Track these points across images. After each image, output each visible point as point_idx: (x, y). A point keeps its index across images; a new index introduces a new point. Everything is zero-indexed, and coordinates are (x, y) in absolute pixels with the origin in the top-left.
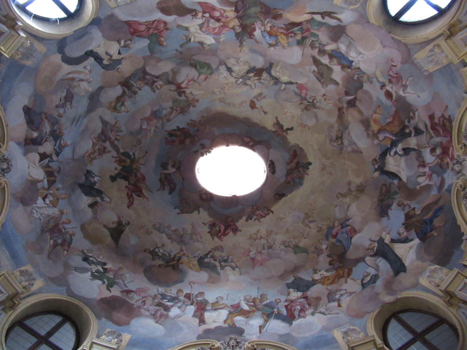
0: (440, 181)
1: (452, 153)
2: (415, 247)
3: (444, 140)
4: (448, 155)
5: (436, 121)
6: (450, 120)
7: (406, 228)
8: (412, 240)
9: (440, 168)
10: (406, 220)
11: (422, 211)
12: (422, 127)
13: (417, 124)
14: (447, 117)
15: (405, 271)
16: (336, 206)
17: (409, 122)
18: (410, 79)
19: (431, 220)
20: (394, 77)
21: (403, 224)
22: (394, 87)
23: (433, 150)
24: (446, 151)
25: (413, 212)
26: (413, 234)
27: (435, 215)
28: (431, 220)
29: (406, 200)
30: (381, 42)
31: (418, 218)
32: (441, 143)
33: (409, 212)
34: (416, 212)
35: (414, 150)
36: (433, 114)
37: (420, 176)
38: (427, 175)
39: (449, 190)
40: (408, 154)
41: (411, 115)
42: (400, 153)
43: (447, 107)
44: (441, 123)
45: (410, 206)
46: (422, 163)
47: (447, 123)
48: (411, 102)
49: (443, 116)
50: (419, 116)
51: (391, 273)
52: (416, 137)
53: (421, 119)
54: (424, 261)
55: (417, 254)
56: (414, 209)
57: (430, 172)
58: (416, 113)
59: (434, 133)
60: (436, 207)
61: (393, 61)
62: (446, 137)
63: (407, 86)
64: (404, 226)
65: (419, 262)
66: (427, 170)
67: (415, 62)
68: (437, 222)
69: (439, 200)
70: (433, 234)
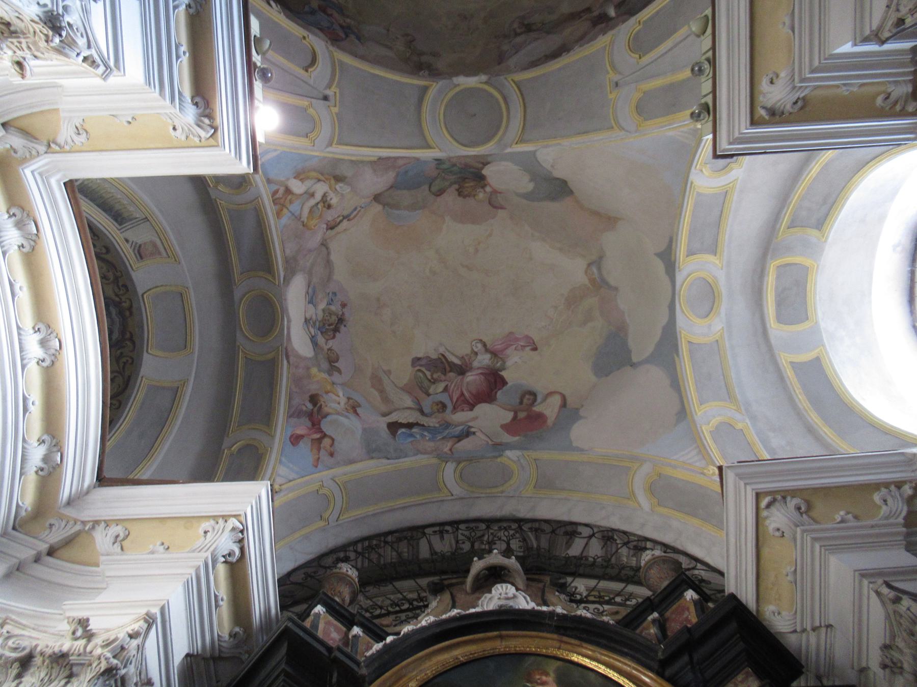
16: (388, 30)
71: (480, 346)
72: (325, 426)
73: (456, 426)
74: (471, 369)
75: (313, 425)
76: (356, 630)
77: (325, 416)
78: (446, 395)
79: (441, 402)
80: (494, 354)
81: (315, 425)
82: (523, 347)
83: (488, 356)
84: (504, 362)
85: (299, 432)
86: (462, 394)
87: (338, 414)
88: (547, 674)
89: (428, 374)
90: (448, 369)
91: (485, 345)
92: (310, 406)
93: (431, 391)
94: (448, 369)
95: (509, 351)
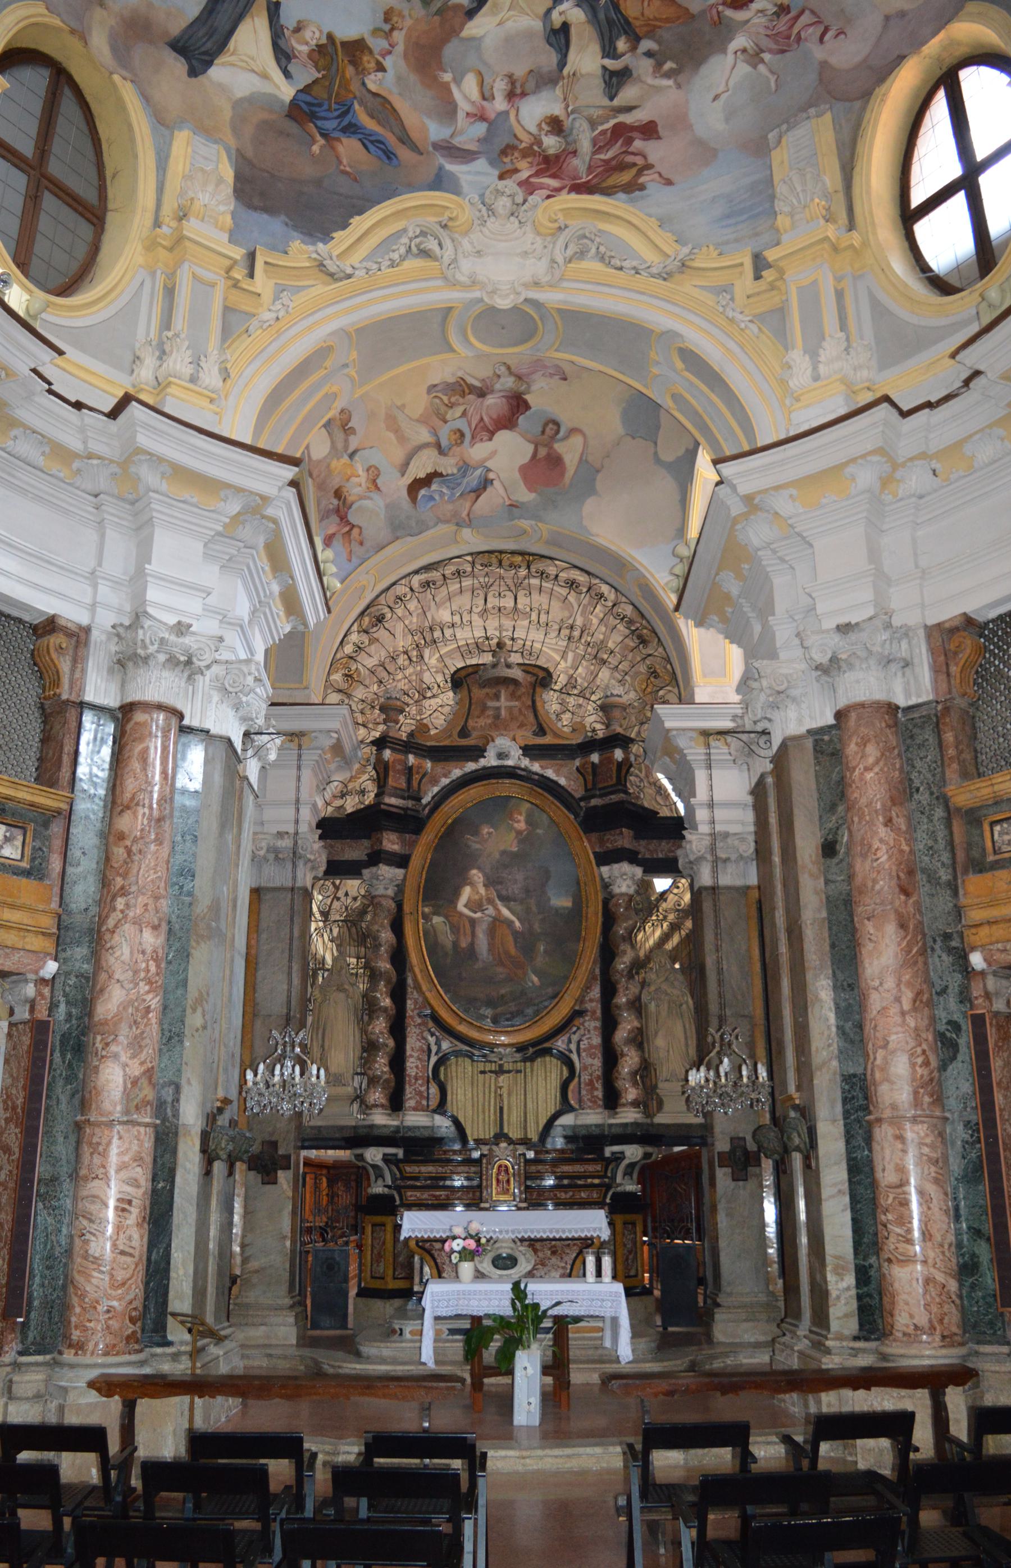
0: (466, 147)
1: (541, 187)
2: (267, 88)
3: (579, 165)
4: (537, 174)
5: (638, 144)
6: (632, 187)
7: (320, 48)
8: (287, 74)
9: (505, 152)
10: (344, 44)
11: (376, 95)
12: (628, 94)
13: (639, 80)
14: (641, 180)
15: (193, 72)
17: (649, 54)
18: (773, 80)
19: (352, 129)
20: (791, 27)
21: (330, 37)
22: (761, 20)
23: (555, 125)
24: (550, 164)
25: (373, 65)
26: (306, 74)
27: (369, 141)
28: (352, 129)
29: (408, 38)
30: (902, 14)
31: (355, 86)
32: (575, 153)
33: (371, 52)
34: (372, 77)
35: (562, 64)
36: (659, 138)
37: (481, 84)
38: (485, 103)
39: (440, 182)
40: (550, 44)
41: (669, 65)
42: (555, 15)
43: (669, 182)
44: (630, 159)
45: (390, 53)
46: (518, 91)
47: (626, 177)
48: (705, 70)
49: (649, 167)
50: (658, 89)
51: (176, 27)
52: (599, 72)
53: (651, 95)
54: (235, 130)
55: (251, 101)
56: (381, 68)
57: (492, 116)
58: (670, 82)
59: (603, 132)
60: (391, 140)
61: (836, 36)
62: (590, 169)
63: (755, 67)
64: (324, 41)
65: (227, 114)
66: (500, 104)
67: (812, 111)
68: (349, 148)
69: (415, 148)
70: (314, 141)
71: (503, 368)
72: (352, 518)
73: (475, 469)
74: (492, 392)
75: (342, 519)
76: (411, 759)
77: (350, 507)
78: (464, 420)
79: (459, 430)
80: (519, 377)
81: (343, 518)
82: (551, 375)
83: (512, 379)
84: (529, 386)
85: (330, 532)
86: (482, 419)
87: (361, 498)
88: (520, 814)
89: (445, 399)
90: (467, 391)
91: (509, 368)
92: (335, 502)
93: (448, 417)
94: (467, 391)
95: (534, 377)
